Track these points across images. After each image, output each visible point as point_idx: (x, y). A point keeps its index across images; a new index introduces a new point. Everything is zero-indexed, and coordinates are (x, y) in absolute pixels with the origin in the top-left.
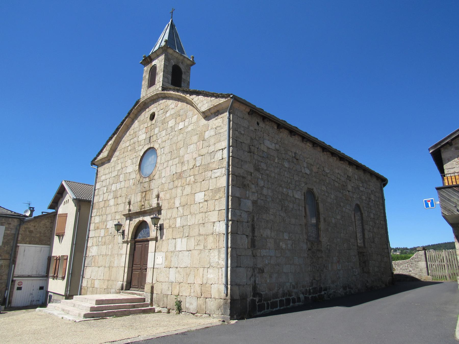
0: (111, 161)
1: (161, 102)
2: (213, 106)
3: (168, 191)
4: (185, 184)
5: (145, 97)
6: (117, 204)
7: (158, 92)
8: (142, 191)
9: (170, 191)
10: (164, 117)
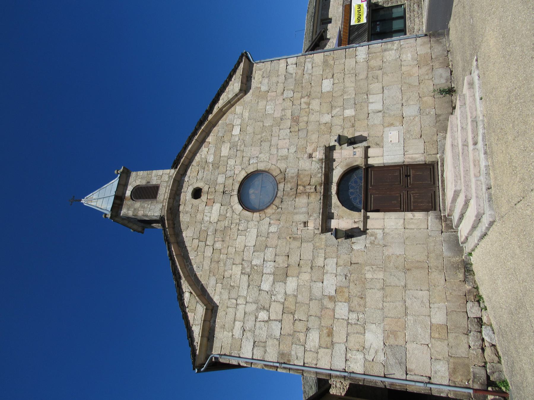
0: (217, 302)
1: (186, 179)
2: (241, 76)
3: (309, 137)
4: (307, 110)
5: (164, 204)
6: (299, 265)
7: (174, 177)
8: (294, 197)
9: (309, 134)
10: (211, 166)
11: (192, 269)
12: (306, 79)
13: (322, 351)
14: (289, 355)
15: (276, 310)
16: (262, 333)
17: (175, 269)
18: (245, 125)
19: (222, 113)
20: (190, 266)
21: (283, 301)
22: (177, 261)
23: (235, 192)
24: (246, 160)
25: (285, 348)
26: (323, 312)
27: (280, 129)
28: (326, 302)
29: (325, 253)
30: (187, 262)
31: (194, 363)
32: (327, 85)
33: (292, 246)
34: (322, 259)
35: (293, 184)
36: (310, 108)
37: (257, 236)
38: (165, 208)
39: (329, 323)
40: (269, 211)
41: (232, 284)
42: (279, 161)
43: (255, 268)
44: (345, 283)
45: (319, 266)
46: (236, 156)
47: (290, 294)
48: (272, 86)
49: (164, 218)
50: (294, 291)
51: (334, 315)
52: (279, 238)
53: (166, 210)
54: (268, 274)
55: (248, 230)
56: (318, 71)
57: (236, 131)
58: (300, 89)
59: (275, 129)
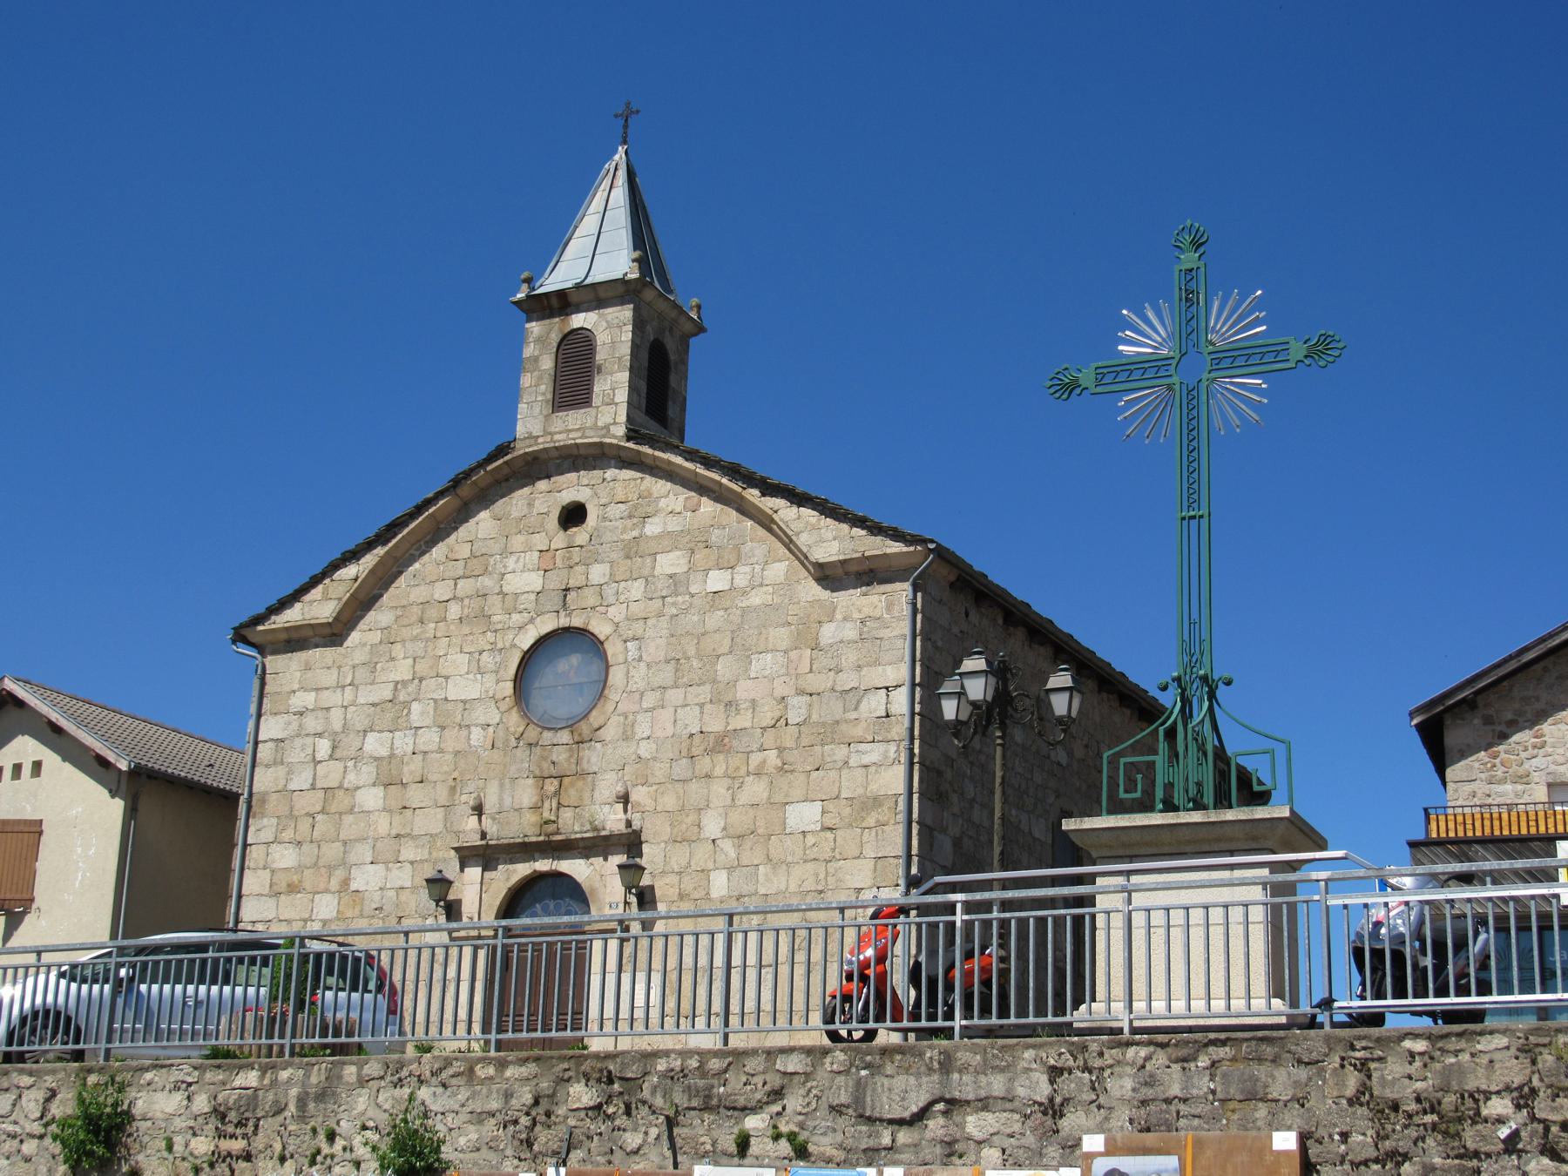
0: (349, 642)
1: (611, 473)
2: (859, 555)
3: (670, 786)
4: (743, 771)
5: (540, 440)
6: (405, 808)
7: (608, 440)
8: (537, 773)
9: (679, 786)
10: (635, 533)
11: (412, 560)
12: (834, 754)
13: (266, 874)
14: (262, 813)
15: (330, 774)
16: (296, 754)
17: (404, 521)
18: (728, 603)
19: (766, 522)
20: (417, 553)
21: (345, 786)
22: (417, 522)
23: (564, 622)
24: (638, 628)
25: (273, 802)
26: (323, 870)
27: (702, 705)
28: (339, 874)
29: (422, 861)
30: (426, 542)
31: (242, 626)
32: (804, 815)
33: (439, 786)
34: (411, 857)
35: (566, 765)
36: (747, 779)
37: (464, 702)
38: (530, 446)
39: (307, 885)
40: (514, 720)
41: (379, 666)
42: (622, 719)
43: (405, 711)
44: (369, 907)
45: (399, 851)
46: (651, 599)
47: (356, 798)
48: (829, 655)
49: (506, 455)
50: (360, 806)
51: (319, 893)
52: (457, 753)
53: (527, 450)
54: (393, 743)
55: (479, 676)
56: (851, 785)
57: (717, 580)
58: (805, 741)
59: (704, 692)
